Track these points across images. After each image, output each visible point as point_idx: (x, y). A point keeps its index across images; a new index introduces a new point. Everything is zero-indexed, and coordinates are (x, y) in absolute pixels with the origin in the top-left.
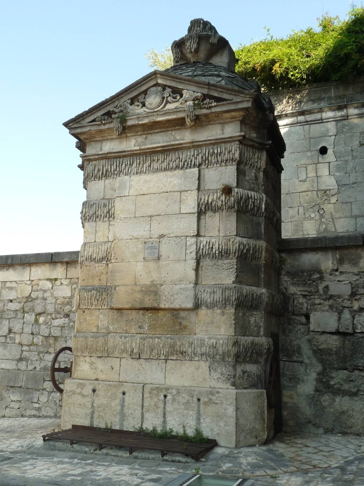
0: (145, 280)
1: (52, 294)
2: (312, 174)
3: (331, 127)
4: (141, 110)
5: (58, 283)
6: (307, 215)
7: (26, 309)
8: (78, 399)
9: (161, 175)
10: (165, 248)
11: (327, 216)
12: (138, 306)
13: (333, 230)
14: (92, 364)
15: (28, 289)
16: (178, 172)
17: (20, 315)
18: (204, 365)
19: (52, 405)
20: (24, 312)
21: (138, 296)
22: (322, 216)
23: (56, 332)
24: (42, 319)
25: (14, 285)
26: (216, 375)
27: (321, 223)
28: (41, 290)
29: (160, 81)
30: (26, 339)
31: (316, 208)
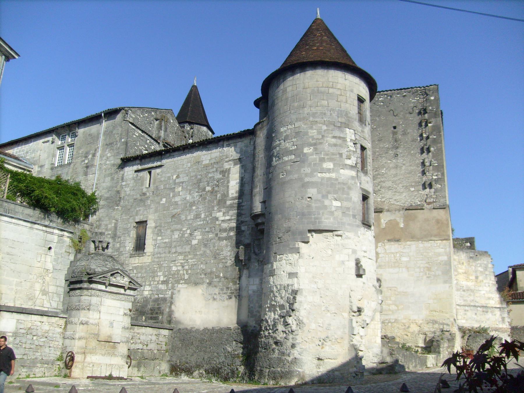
0: (109, 334)
1: (41, 328)
2: (43, 259)
3: (56, 238)
4: (114, 279)
5: (44, 323)
6: (37, 280)
7: (28, 333)
8: (88, 368)
9: (115, 301)
10: (115, 324)
11: (46, 283)
12: (106, 341)
13: (47, 290)
14: (91, 357)
15: (29, 325)
16: (119, 301)
17: (25, 335)
18: (120, 358)
19: (41, 372)
20: (27, 334)
21: (107, 338)
22: (44, 282)
23: (42, 344)
24: (35, 338)
25: (23, 322)
26: (123, 361)
27: (43, 286)
28: (36, 325)
29: (119, 271)
30: (28, 346)
31: (42, 277)
